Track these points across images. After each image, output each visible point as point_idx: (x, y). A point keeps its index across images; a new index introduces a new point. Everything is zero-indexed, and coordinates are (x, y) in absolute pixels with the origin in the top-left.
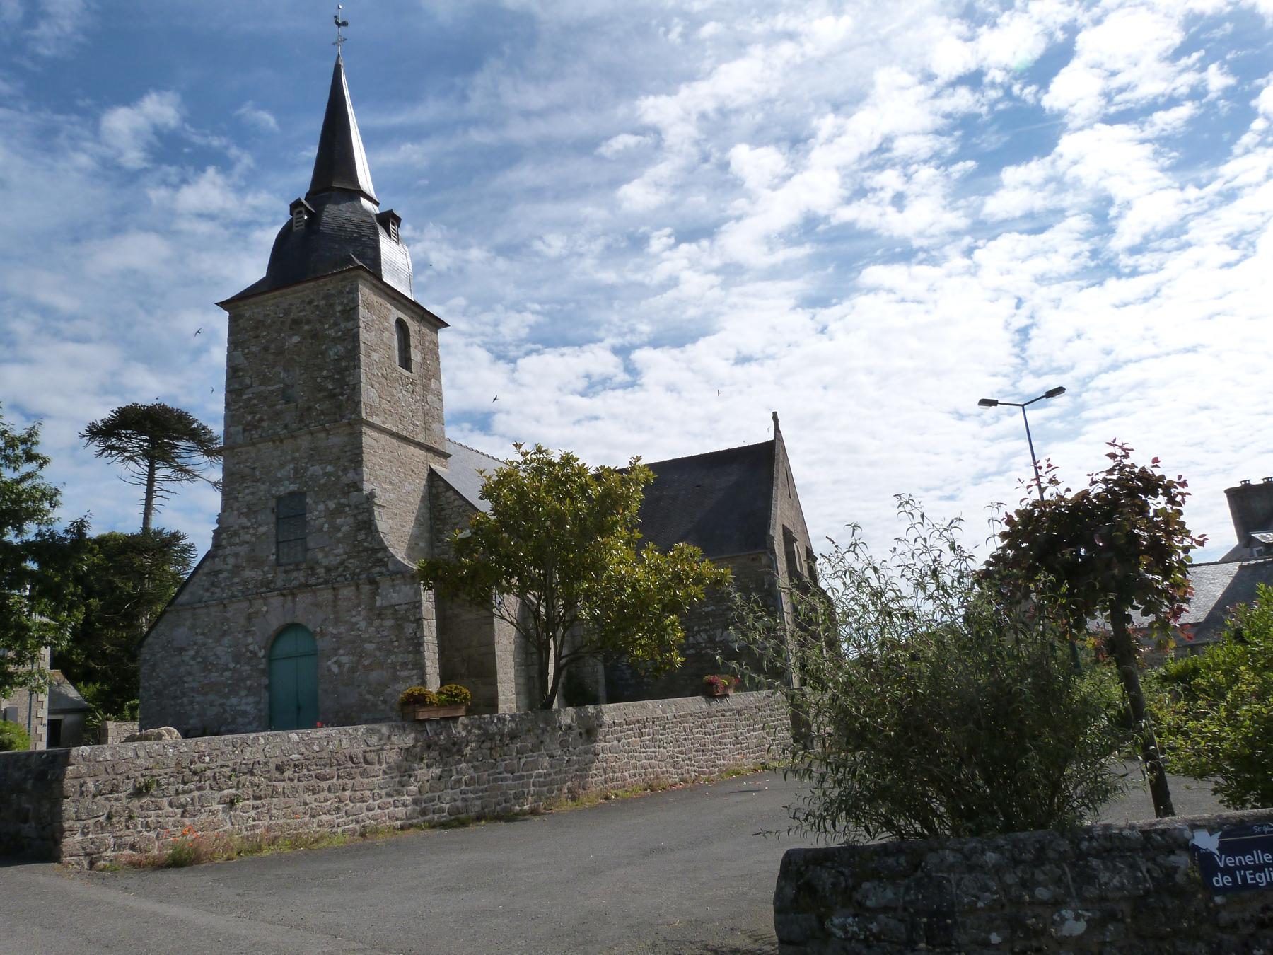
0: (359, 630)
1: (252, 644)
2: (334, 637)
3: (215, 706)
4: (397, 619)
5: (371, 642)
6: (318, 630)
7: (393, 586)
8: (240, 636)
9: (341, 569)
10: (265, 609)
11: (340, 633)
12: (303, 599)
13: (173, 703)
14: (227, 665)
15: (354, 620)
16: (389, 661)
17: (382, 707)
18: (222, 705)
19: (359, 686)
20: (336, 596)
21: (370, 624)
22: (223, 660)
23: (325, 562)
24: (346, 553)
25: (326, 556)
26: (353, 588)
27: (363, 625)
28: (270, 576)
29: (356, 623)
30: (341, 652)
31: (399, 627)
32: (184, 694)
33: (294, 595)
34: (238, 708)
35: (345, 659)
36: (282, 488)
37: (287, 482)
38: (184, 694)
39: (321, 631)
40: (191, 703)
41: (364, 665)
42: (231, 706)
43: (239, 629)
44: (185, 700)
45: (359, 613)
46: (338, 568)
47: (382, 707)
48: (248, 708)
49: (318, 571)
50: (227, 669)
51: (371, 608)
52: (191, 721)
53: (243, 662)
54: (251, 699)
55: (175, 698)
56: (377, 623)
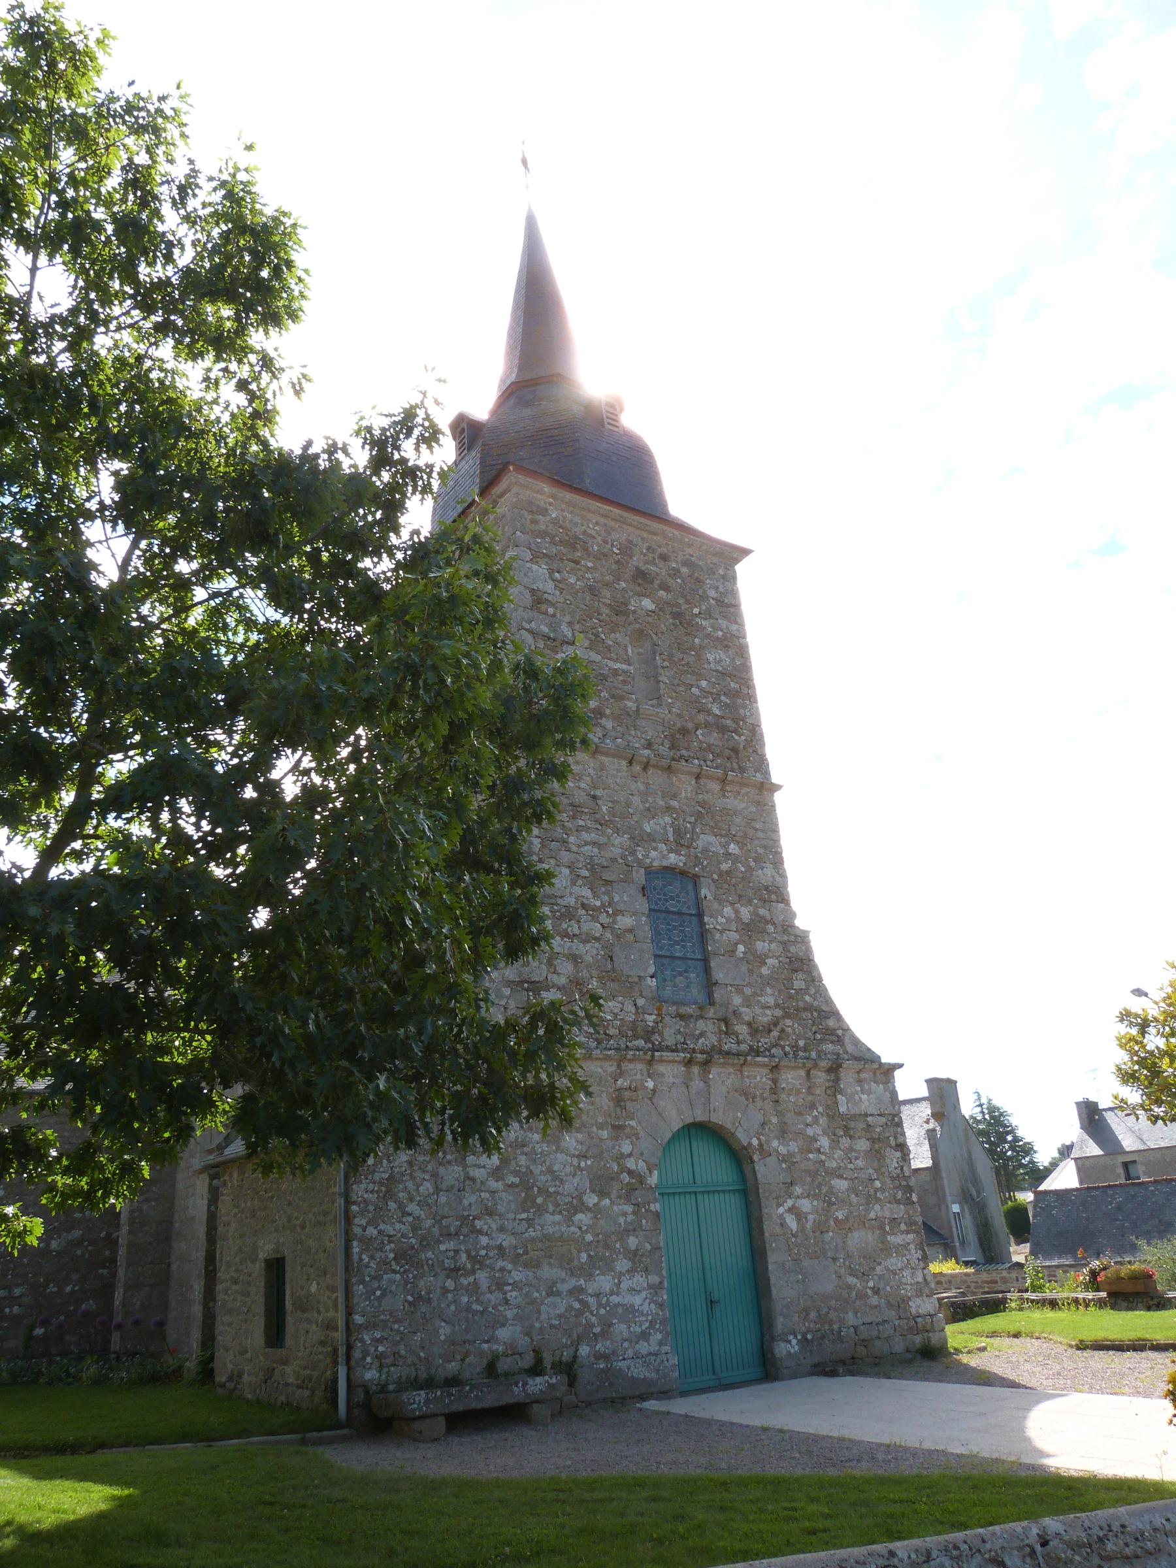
0: (819, 1151)
1: (630, 1155)
2: (784, 1161)
3: (558, 1294)
4: (873, 1141)
5: (841, 1177)
6: (755, 1142)
7: (860, 1081)
8: (605, 1134)
9: (775, 1034)
10: (650, 1084)
11: (791, 1155)
12: (722, 1077)
13: (450, 1284)
14: (580, 1197)
15: (810, 1132)
16: (872, 1215)
17: (874, 1300)
18: (576, 1291)
19: (834, 1259)
20: (775, 1081)
21: (835, 1144)
22: (569, 1187)
23: (747, 1013)
24: (777, 1006)
25: (747, 1003)
26: (803, 1073)
27: (824, 1142)
28: (650, 1019)
29: (814, 1139)
30: (798, 1190)
31: (876, 1155)
32: (478, 1262)
33: (706, 1064)
34: (615, 1299)
35: (805, 1205)
36: (653, 854)
37: (662, 847)
38: (478, 1262)
39: (761, 1145)
40: (499, 1285)
41: (836, 1220)
42: (597, 1295)
43: (600, 1120)
44: (482, 1276)
45: (816, 1120)
46: (770, 1031)
47: (874, 1300)
48: (637, 1300)
49: (737, 1028)
50: (581, 1207)
51: (833, 1115)
52: (503, 1334)
53: (614, 1193)
54: (639, 1280)
55: (454, 1272)
56: (845, 1142)
